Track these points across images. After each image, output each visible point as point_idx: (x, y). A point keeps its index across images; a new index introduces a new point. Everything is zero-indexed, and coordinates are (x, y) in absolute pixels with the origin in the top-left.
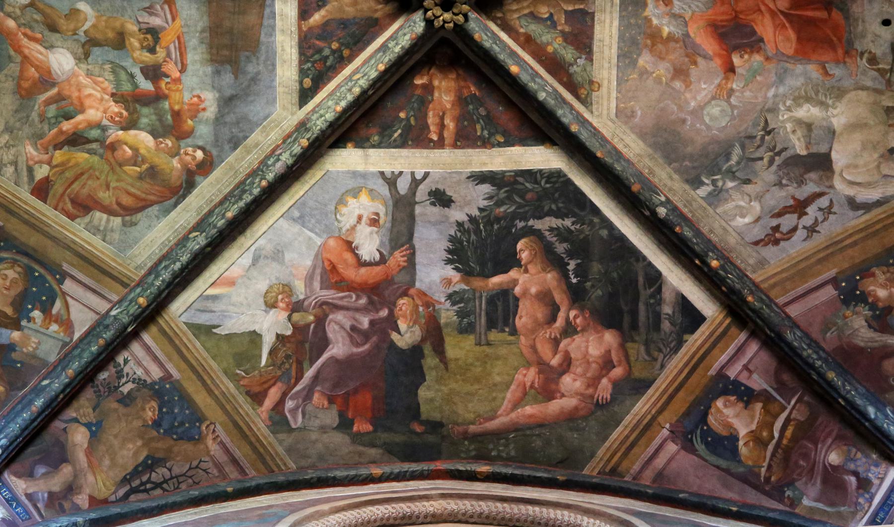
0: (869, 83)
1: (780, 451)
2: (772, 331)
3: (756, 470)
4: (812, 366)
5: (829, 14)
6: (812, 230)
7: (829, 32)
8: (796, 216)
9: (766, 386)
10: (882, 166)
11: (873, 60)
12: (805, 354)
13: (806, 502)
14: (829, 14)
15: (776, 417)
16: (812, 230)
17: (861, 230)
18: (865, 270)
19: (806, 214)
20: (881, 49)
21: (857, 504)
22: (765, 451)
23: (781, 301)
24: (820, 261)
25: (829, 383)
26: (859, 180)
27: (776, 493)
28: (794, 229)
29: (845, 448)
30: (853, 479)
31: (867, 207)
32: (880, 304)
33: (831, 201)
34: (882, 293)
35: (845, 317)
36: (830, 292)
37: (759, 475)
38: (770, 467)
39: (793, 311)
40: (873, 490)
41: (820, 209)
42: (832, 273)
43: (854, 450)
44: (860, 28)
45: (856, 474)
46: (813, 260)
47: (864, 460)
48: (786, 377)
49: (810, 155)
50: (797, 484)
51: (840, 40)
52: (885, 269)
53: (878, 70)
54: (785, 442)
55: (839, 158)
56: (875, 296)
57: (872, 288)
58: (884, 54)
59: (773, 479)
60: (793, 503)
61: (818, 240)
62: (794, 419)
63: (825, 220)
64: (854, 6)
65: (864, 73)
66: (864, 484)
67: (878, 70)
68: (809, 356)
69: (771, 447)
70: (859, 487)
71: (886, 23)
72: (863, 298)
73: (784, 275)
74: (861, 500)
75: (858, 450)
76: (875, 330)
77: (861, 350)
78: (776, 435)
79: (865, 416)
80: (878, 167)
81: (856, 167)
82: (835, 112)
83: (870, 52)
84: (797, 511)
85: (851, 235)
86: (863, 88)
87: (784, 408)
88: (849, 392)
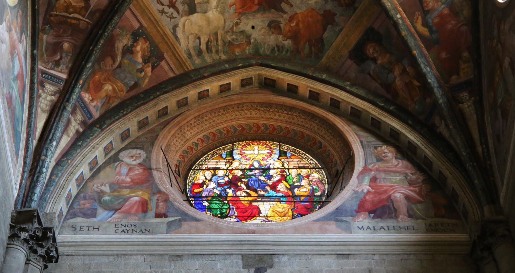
0: (227, 24)
1: (65, 19)
2: (117, 9)
3: (55, 9)
4: (104, 31)
5: (256, 5)
6: (163, 12)
7: (249, 5)
8: (168, 4)
9: (92, 6)
10: (192, 35)
11: (237, 24)
12: (110, 27)
13: (45, 37)
14: (256, 5)
15: (80, 14)
16: (163, 12)
17: (164, 33)
18: (147, 38)
19: (169, 8)
20: (242, 27)
21: (48, 62)
22: (64, 12)
23: (131, 6)
24: (150, 18)
25: (98, 41)
26: (186, 27)
27: (47, 22)
28: (162, 4)
29: (71, 50)
30: (58, 57)
31: (174, 33)
32: (134, 49)
33: (176, 18)
34: (138, 48)
35: (126, 35)
36: (136, 25)
37: (53, 11)
38: (57, 15)
39: (128, 13)
40: (56, 69)
41: (172, 14)
42: (145, 25)
43: (71, 55)
44: (250, 17)
45: (61, 58)
46: (150, 15)
47: (68, 61)
48: (97, 14)
49: (195, 5)
50: (52, 31)
51: (246, 10)
52: (149, 47)
53: (233, 27)
54: (69, 20)
55: (195, 17)
56: (137, 45)
57: (140, 43)
58: (240, 28)
59: (52, 18)
60: (44, 31)
61: (158, 16)
62: (80, 23)
63: (168, 17)
64: (260, 15)
65: (231, 21)
66: (57, 64)
67: (233, 27)
68: (109, 29)
69: (65, 14)
70: (56, 61)
71: (253, 27)
72: (135, 41)
73: (142, 4)
74: (50, 63)
75: (71, 57)
76: (122, 50)
77: (113, 46)
78: (71, 15)
79: (87, 62)
80: (192, 34)
81: (191, 25)
82: (214, 12)
83: (240, 23)
84: (40, 33)
85: (162, 29)
86: (225, 22)
87: (83, 16)
88: (96, 52)
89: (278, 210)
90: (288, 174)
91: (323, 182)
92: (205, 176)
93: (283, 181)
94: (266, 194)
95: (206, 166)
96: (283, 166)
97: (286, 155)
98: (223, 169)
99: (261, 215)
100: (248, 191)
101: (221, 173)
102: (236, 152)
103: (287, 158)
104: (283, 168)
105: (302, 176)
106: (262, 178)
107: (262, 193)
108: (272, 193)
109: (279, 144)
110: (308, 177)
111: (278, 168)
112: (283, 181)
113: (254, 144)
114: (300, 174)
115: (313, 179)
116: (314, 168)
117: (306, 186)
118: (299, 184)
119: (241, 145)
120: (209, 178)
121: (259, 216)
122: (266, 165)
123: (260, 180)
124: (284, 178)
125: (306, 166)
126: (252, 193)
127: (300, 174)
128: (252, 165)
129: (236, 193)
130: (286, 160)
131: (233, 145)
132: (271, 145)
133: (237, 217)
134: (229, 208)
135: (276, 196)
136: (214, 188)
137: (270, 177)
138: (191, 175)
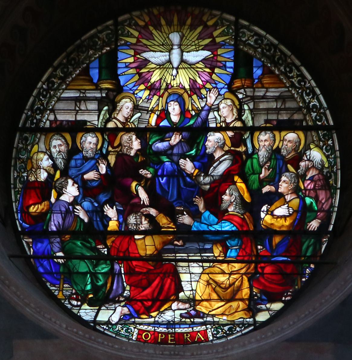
89: (221, 278)
90: (250, 151)
91: (331, 182)
92: (51, 157)
93: (236, 178)
94: (196, 227)
95: (52, 117)
96: (239, 118)
97: (250, 75)
98: (94, 130)
99: (181, 295)
100: (153, 212)
101: (90, 142)
102: (126, 58)
103: (252, 86)
104: (238, 124)
105: (283, 157)
106: (188, 166)
107: (186, 219)
108: (210, 222)
109: (236, 23)
110: (296, 161)
111: (227, 128)
112: (236, 178)
113: (169, 24)
114: (278, 150)
115: (308, 169)
116: (316, 128)
117: (288, 198)
118: (273, 188)
119: (136, 26)
120: (60, 162)
121: (177, 299)
122: (199, 112)
123: (181, 172)
124: (240, 164)
125: (296, 117)
126: (163, 221)
127: (278, 150)
128: (165, 114)
129: (125, 220)
130: (249, 92)
131: (116, 24)
132: (215, 26)
133: (129, 301)
134: (111, 273)
135: (217, 233)
136: (76, 202)
137: (205, 161)
138: (19, 151)
